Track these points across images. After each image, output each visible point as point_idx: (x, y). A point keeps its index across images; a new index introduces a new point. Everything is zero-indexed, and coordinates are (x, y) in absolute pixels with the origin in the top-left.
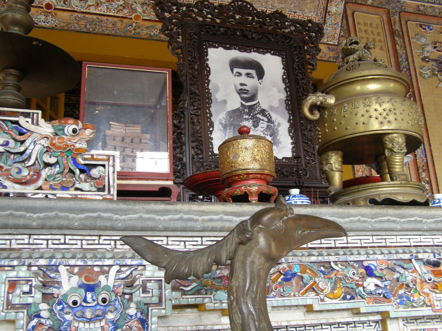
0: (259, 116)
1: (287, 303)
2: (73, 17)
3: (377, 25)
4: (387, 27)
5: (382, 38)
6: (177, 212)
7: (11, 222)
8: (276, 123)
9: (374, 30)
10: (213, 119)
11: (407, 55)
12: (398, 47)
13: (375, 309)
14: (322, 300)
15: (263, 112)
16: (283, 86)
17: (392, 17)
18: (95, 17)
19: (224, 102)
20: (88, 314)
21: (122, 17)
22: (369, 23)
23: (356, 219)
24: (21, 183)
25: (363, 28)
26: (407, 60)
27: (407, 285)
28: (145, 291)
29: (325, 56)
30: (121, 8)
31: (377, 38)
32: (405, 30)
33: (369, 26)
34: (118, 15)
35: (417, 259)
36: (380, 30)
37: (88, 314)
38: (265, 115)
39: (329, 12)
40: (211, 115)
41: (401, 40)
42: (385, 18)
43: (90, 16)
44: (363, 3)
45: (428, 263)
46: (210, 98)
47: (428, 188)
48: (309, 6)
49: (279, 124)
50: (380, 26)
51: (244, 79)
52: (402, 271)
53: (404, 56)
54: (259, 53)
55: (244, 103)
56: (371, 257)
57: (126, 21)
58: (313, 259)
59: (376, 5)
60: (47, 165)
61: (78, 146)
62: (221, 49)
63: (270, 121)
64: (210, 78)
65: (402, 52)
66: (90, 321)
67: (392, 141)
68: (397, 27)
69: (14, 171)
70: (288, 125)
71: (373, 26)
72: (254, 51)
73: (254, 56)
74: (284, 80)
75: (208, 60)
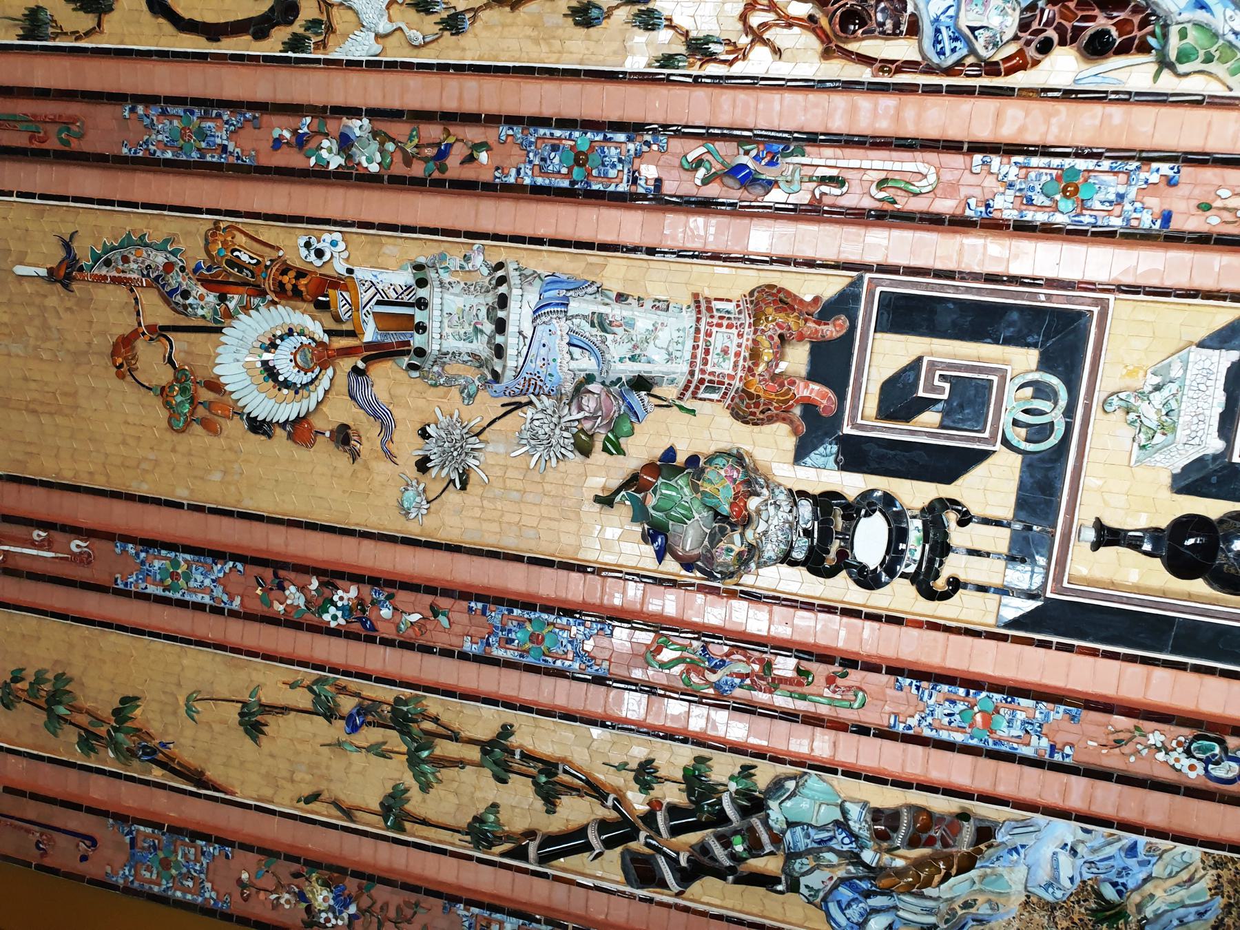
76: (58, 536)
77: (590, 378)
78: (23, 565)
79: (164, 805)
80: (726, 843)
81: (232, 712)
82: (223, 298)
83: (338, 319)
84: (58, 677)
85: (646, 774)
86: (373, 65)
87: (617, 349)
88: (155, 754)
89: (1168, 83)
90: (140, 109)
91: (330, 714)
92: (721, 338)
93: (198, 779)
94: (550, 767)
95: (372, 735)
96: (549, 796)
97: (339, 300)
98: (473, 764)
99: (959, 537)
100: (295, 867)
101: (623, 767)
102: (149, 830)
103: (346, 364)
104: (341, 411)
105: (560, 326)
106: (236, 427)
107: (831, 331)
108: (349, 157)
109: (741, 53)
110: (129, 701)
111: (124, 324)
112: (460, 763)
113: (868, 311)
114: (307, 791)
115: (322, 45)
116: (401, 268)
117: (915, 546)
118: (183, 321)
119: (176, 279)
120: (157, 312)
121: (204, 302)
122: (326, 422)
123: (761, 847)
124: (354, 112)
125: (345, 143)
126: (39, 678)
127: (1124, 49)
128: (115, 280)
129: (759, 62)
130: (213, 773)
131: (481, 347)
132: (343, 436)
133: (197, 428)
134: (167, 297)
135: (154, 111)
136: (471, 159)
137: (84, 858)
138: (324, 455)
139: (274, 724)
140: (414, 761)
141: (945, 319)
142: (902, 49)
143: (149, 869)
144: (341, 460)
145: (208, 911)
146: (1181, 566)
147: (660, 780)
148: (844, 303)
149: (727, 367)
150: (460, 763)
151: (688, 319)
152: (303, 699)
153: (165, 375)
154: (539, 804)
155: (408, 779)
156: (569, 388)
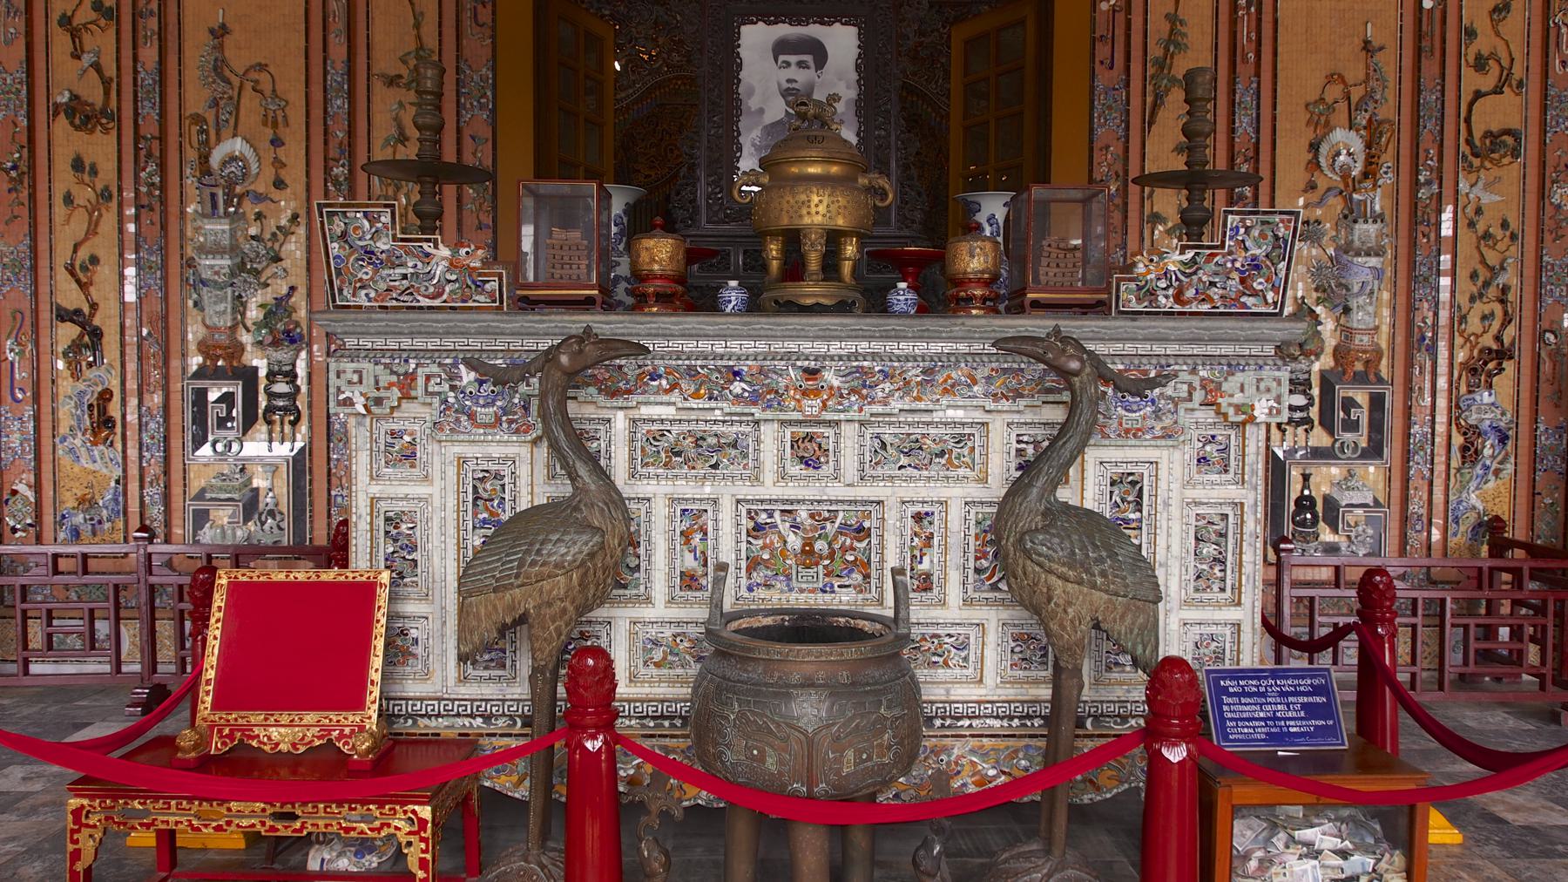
1: (652, 399)
6: (551, 321)
7: (423, 330)
10: (741, 139)
13: (746, 411)
14: (685, 399)
16: (855, 76)
19: (761, 111)
20: (481, 402)
24: (427, 297)
27: (777, 392)
35: (793, 366)
37: (481, 402)
40: (739, 134)
45: (806, 370)
46: (739, 108)
47: (1249, 194)
51: (793, 72)
52: (775, 377)
54: (823, 23)
60: (449, 281)
61: (472, 265)
62: (761, 24)
64: (742, 75)
66: (484, 406)
67: (805, 236)
69: (423, 289)
72: (814, 22)
73: (814, 30)
74: (857, 67)
75: (739, 46)
76: (1254, 45)
77: (1348, 290)
82: (1365, 128)
83: (1360, 182)
86: (1457, 191)
87: (1362, 300)
89: (1453, 472)
90: (1439, 88)
92: (1366, 338)
97: (1368, 184)
99: (1300, 430)
100: (1121, 174)
103: (1342, 187)
104: (1322, 185)
105: (1370, 277)
106: (1310, 135)
107: (1372, 377)
108: (1424, 184)
109: (1461, 334)
111: (1350, 79)
113: (1377, 389)
115: (1464, 170)
116: (1382, 208)
117: (1298, 415)
118: (1353, 107)
119: (1371, 105)
120: (1357, 93)
121: (1362, 119)
122: (1317, 176)
124: (1440, 186)
125: (1428, 183)
126: (1185, 35)
127: (1463, 457)
128: (1367, 75)
129: (1459, 340)
130: (1153, 127)
131: (1357, 243)
132: (1312, 187)
133: (1308, 116)
134: (1361, 99)
135: (1439, 94)
136: (1424, 236)
137: (1102, 63)
138: (1302, 177)
141: (1376, 415)
142: (1463, 389)
144: (1302, 186)
145: (1091, 130)
146: (1298, 502)
148: (1380, 380)
149: (1357, 342)
151: (1371, 326)
153: (1329, 100)
155: (1170, 224)
156: (1343, 281)
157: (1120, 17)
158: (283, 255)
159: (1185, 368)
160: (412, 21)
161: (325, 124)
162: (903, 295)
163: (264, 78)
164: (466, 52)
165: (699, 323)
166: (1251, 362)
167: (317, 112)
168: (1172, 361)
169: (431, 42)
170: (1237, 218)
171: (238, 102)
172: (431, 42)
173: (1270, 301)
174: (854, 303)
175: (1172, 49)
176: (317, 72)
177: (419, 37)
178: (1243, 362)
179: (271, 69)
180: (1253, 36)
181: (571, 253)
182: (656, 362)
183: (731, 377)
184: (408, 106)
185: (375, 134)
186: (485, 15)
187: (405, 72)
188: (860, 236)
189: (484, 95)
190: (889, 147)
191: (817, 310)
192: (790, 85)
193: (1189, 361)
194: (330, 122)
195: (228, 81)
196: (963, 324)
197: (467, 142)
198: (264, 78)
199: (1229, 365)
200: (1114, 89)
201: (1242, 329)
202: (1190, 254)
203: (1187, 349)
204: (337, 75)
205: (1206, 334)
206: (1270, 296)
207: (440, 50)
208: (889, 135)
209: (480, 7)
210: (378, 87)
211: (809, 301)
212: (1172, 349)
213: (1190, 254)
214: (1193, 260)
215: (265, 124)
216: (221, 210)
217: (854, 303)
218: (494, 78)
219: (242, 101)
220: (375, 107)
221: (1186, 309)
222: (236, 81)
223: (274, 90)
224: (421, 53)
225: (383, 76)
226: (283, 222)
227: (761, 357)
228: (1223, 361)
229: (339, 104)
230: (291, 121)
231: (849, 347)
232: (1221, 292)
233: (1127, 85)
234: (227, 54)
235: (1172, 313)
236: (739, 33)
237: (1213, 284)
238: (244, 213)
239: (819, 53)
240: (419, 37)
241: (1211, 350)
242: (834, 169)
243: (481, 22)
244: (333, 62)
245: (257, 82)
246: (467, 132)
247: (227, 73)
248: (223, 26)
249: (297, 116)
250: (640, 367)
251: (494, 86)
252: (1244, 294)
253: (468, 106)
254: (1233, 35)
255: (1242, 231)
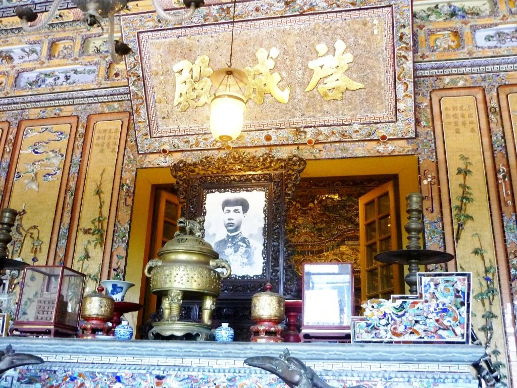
0: (240, 243)
2: (183, 155)
3: (469, 106)
4: (481, 106)
5: (475, 119)
6: (22, 343)
8: (253, 248)
9: (464, 112)
11: (504, 132)
12: (492, 125)
15: (244, 240)
17: (488, 93)
18: (199, 152)
19: (214, 235)
21: (217, 149)
22: (459, 105)
23: (113, 348)
25: (451, 113)
26: (504, 137)
28: (6, 381)
29: (403, 150)
30: (215, 142)
31: (468, 120)
32: (503, 104)
33: (459, 109)
34: (214, 148)
36: (474, 111)
38: (245, 242)
39: (399, 110)
41: (498, 117)
42: (480, 96)
43: (196, 152)
44: (453, 86)
48: (378, 107)
49: (255, 248)
50: (474, 107)
51: (232, 215)
53: (500, 134)
54: (248, 191)
55: (229, 234)
56: (121, 370)
57: (221, 151)
58: (87, 370)
59: (468, 85)
63: (248, 246)
65: (498, 130)
68: (494, 104)
70: (262, 248)
71: (464, 109)
73: (242, 195)
74: (265, 211)
75: (205, 204)
76: (510, 197)
78: (500, 188)
79: (448, 229)
80: (487, 374)
81: (478, 246)
84: (472, 200)
85: (496, 352)
88: (460, 226)
91: (487, 271)
93: (458, 239)
94: (491, 329)
95: (484, 283)
96: (483, 329)
98: (485, 310)
101: (496, 347)
102: (441, 226)
110: (472, 218)
112: (484, 305)
114: (464, 267)
123: (489, 382)
126: (470, 194)
130: (460, 241)
137: (427, 209)
139: (478, 257)
140: (481, 294)
143: (430, 227)
147: (496, 356)
150: (484, 305)
152: (488, 265)
154: (480, 327)
157: (435, 187)
158: (28, 312)
159: (402, 380)
160: (99, 205)
161: (56, 251)
162: (225, 331)
163: (35, 232)
164: (120, 218)
165: (99, 346)
166: (450, 376)
167: (53, 246)
168: (393, 375)
169: (105, 213)
170: (429, 279)
171: (23, 242)
172: (105, 213)
173: (459, 333)
174: (198, 335)
175: (464, 201)
176: (57, 228)
177: (101, 212)
178: (443, 376)
179: (39, 228)
180: (509, 192)
181: (49, 305)
182: (74, 369)
183: (115, 380)
184: (92, 242)
185: (76, 255)
186: (129, 201)
187: (93, 227)
188: (215, 296)
189: (125, 236)
190: (278, 251)
191: (172, 338)
192: (230, 222)
193: (405, 375)
194: (58, 250)
195: (20, 234)
196: (251, 348)
197: (115, 258)
198: (35, 232)
199: (434, 379)
200: (436, 222)
201: (438, 353)
202: (399, 302)
203: (404, 367)
204: (64, 229)
205: (415, 357)
206: (459, 330)
207: (109, 217)
208: (279, 245)
209: (128, 198)
210: (81, 233)
211: (168, 333)
212: (395, 367)
213: (399, 302)
214: (402, 307)
215: (32, 252)
216: (6, 293)
217: (198, 335)
218: (130, 229)
219: (25, 242)
220: (78, 243)
221: (401, 339)
222: (24, 233)
223: (38, 237)
224: (101, 219)
225: (84, 229)
226: (31, 297)
227: (133, 367)
228: (430, 375)
229: (63, 242)
230: (43, 250)
231: (187, 362)
232: (424, 327)
233: (442, 220)
234: (23, 222)
235: (391, 342)
236: (206, 198)
237: (417, 322)
238: (16, 292)
239: (245, 205)
240: (101, 212)
241: (422, 367)
242: (194, 258)
243: (127, 204)
244: (64, 224)
245: (32, 234)
246: (115, 254)
247: (21, 230)
248: (24, 211)
249: (45, 248)
250: (65, 372)
251: (129, 232)
252: (440, 329)
253: (117, 241)
254: (498, 192)
255: (433, 286)
